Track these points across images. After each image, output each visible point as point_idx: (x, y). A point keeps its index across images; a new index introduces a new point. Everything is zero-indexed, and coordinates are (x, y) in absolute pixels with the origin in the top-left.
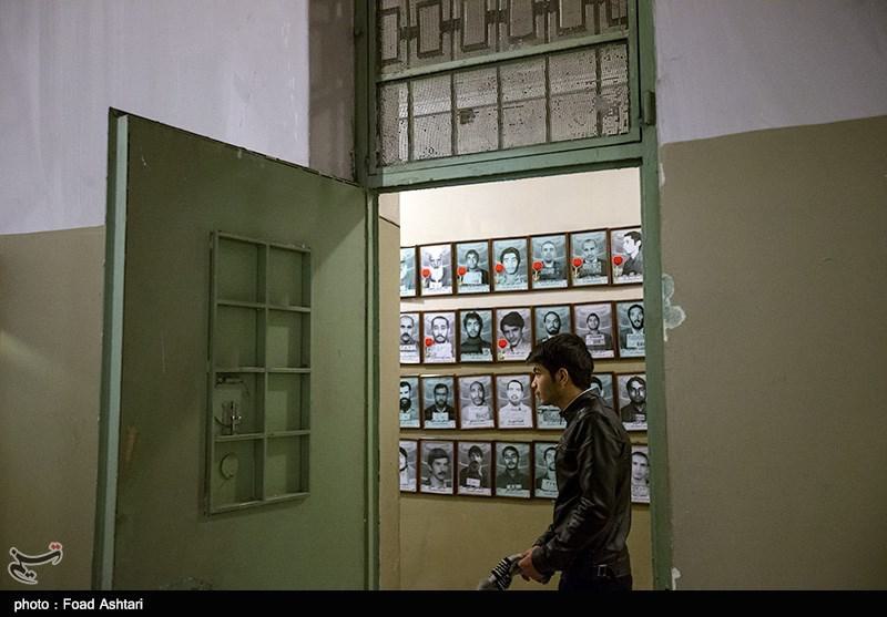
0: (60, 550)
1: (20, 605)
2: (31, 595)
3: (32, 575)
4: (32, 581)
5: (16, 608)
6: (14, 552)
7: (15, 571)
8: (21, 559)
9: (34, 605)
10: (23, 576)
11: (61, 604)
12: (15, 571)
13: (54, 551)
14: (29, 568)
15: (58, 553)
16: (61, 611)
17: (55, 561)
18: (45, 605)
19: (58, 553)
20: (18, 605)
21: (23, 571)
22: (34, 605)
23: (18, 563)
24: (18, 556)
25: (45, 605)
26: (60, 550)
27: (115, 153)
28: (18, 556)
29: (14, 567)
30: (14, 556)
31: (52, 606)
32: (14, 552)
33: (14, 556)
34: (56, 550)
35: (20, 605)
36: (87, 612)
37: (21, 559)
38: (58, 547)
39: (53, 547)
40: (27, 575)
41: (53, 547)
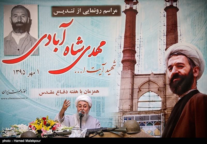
1: (4, 141)
5: (3, 142)
6: (3, 129)
7: (3, 133)
8: (5, 130)
9: (7, 141)
11: (13, 141)
12: (3, 133)
16: (13, 143)
18: (10, 141)
22: (7, 141)
25: (10, 141)
31: (11, 141)
32: (3, 129)
35: (4, 141)
36: (22, 143)
37: (5, 130)
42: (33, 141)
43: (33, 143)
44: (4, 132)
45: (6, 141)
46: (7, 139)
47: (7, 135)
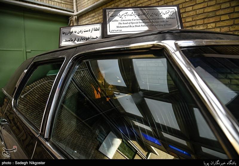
0: (16, 148)
1: (3, 163)
2: (7, 160)
3: (9, 155)
4: (8, 156)
5: (2, 164)
6: (4, 148)
7: (4, 154)
9: (7, 163)
10: (7, 155)
13: (14, 148)
14: (8, 153)
15: (16, 149)
17: (15, 151)
18: (10, 163)
19: (16, 149)
20: (3, 163)
21: (6, 154)
22: (7, 163)
23: (7, 152)
24: (5, 150)
26: (16, 148)
27: (41, 6)
28: (5, 150)
29: (4, 153)
30: (4, 150)
31: (12, 163)
32: (4, 148)
33: (4, 150)
34: (15, 148)
35: (3, 163)
38: (16, 147)
39: (14, 147)
40: (7, 155)
41: (14, 147)
42: (34, 163)
43: (34, 165)
44: (5, 153)
45: (6, 163)
46: (7, 160)
47: (9, 156)
